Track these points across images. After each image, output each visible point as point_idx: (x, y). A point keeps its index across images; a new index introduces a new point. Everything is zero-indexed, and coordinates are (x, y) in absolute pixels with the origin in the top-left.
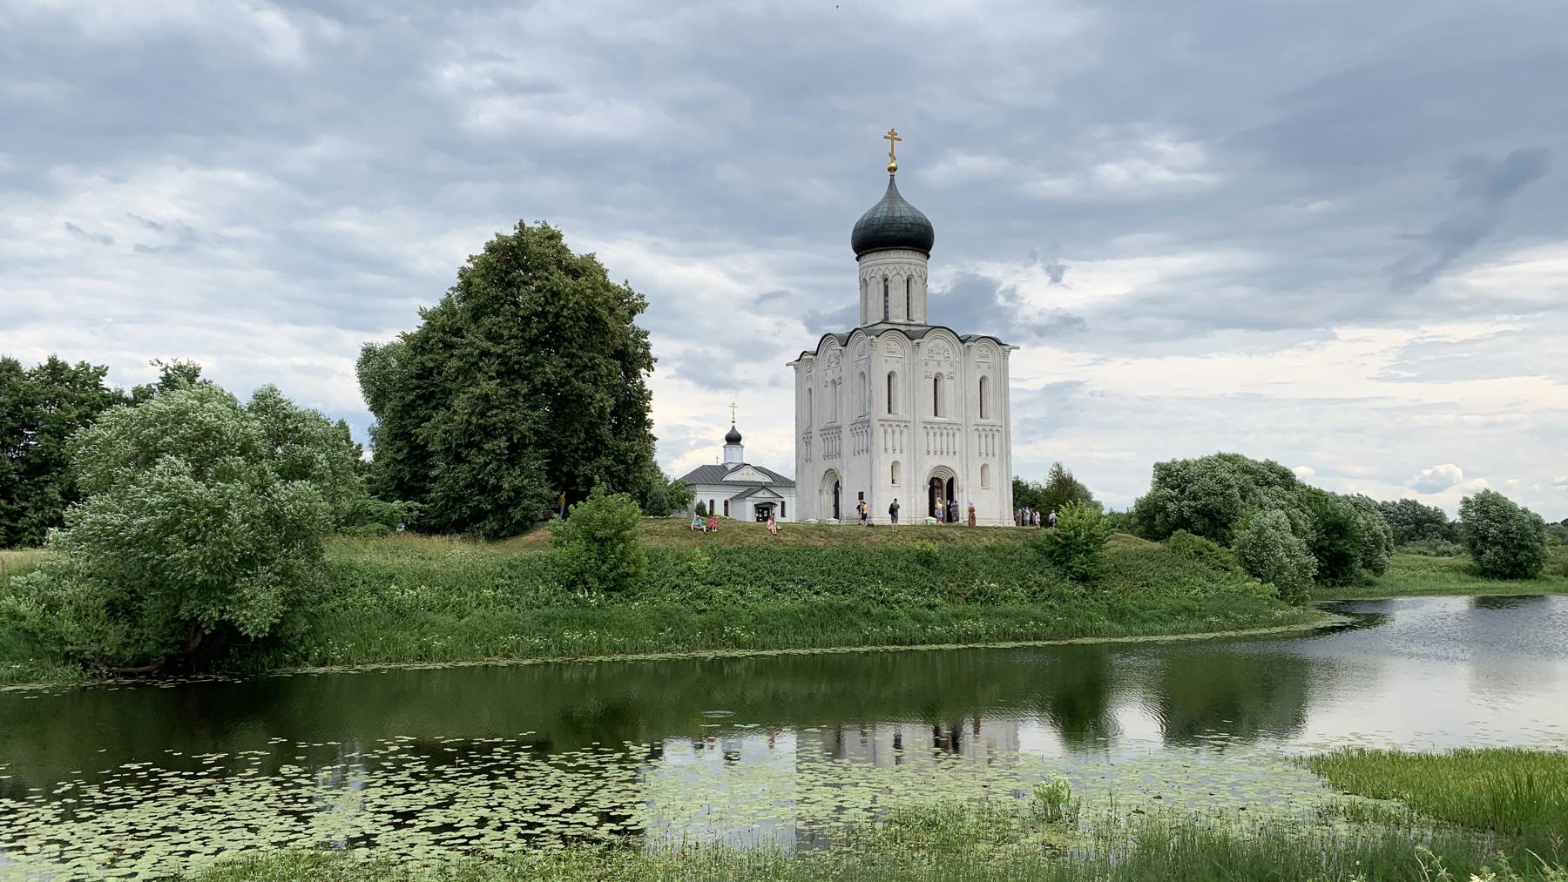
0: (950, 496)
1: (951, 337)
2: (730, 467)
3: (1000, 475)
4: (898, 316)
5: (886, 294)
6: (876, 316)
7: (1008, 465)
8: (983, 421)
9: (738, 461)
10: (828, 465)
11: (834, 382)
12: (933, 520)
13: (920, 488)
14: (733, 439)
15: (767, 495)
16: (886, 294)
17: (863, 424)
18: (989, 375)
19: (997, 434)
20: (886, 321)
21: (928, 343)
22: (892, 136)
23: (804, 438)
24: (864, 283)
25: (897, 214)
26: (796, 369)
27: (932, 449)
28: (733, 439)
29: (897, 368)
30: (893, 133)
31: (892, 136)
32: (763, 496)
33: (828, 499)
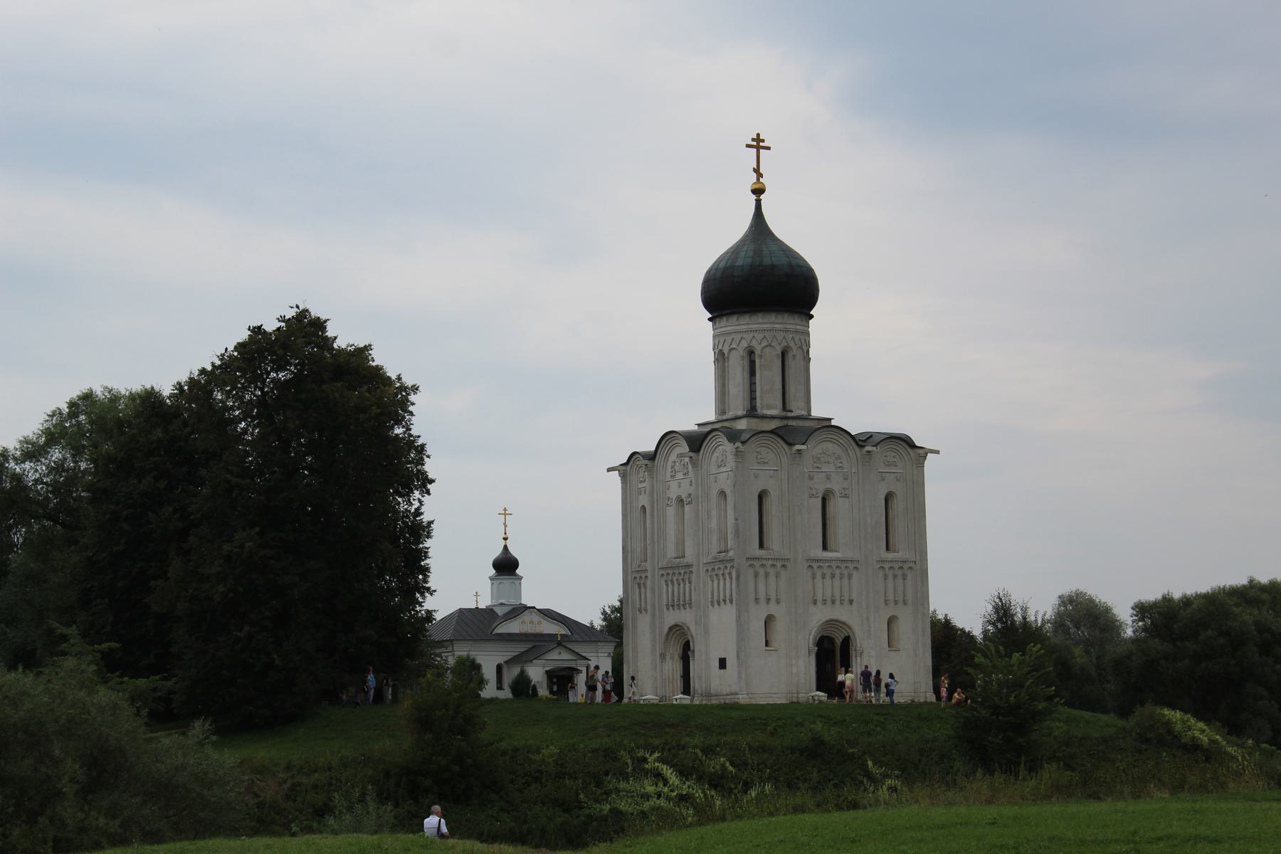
1: (844, 440)
2: (500, 611)
4: (770, 404)
5: (752, 373)
6: (738, 406)
8: (890, 556)
9: (513, 601)
10: (672, 618)
11: (680, 501)
12: (822, 695)
13: (804, 652)
14: (506, 566)
15: (566, 656)
16: (752, 373)
19: (910, 570)
20: (752, 412)
21: (812, 448)
22: (758, 144)
24: (721, 358)
25: (767, 261)
26: (624, 477)
27: (819, 596)
28: (506, 566)
30: (758, 139)
31: (758, 144)
32: (559, 658)
33: (673, 667)
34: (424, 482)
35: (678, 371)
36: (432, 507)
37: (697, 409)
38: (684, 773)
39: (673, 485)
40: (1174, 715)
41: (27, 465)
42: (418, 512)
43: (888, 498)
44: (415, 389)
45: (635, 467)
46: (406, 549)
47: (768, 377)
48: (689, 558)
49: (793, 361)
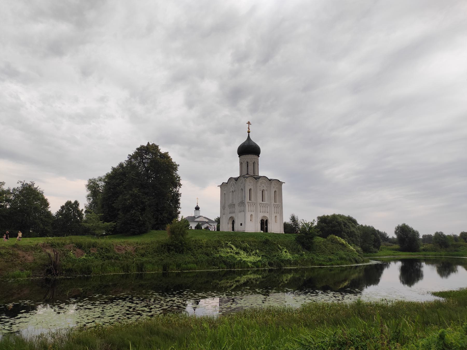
0: (267, 225)
2: (196, 217)
3: (280, 219)
4: (251, 173)
5: (248, 166)
6: (245, 173)
7: (282, 216)
9: (198, 215)
11: (233, 191)
12: (262, 232)
14: (197, 208)
15: (208, 225)
16: (248, 166)
17: (242, 203)
18: (277, 190)
19: (279, 207)
20: (248, 174)
21: (260, 181)
22: (249, 123)
23: (223, 207)
28: (197, 208)
29: (252, 188)
31: (249, 123)
33: (230, 226)
34: (180, 185)
35: (233, 167)
36: (181, 190)
37: (237, 174)
38: (237, 247)
39: (231, 188)
40: (337, 237)
41: (100, 182)
42: (178, 191)
43: (275, 191)
44: (179, 165)
45: (223, 186)
46: (175, 200)
47: (251, 167)
48: (234, 203)
49: (255, 165)
